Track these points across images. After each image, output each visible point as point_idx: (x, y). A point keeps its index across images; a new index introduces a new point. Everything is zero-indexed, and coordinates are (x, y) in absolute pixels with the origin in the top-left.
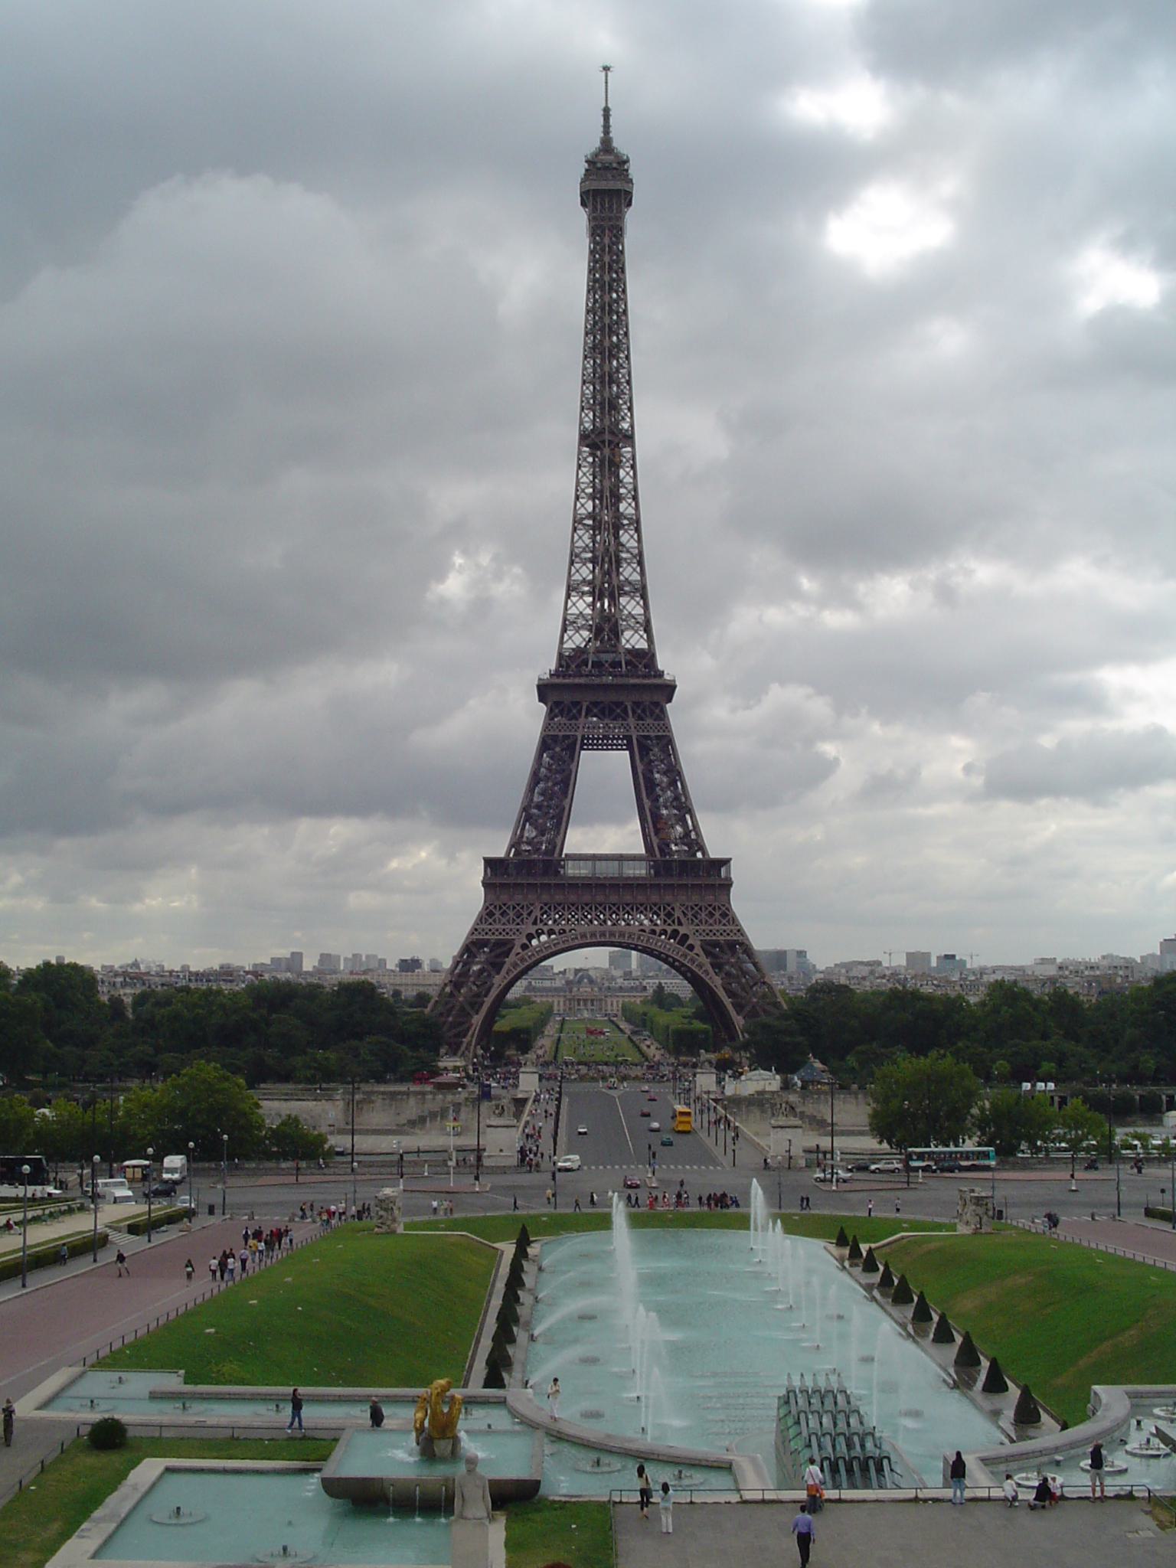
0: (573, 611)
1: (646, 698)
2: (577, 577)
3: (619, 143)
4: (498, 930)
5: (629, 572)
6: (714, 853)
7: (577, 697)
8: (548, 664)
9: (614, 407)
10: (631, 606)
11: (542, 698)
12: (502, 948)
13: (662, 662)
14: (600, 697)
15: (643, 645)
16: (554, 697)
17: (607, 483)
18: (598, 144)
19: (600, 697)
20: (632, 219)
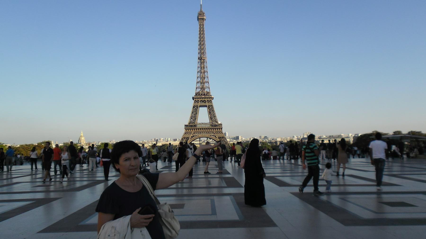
0: (198, 86)
1: (209, 99)
2: (198, 81)
3: (204, 11)
4: (187, 136)
5: (206, 80)
6: (219, 122)
7: (198, 99)
8: (194, 95)
9: (203, 53)
10: (206, 85)
11: (193, 99)
12: (188, 138)
13: (211, 94)
14: (202, 99)
15: (208, 91)
16: (195, 99)
17: (202, 66)
18: (199, 10)
19: (202, 99)
20: (205, 23)
